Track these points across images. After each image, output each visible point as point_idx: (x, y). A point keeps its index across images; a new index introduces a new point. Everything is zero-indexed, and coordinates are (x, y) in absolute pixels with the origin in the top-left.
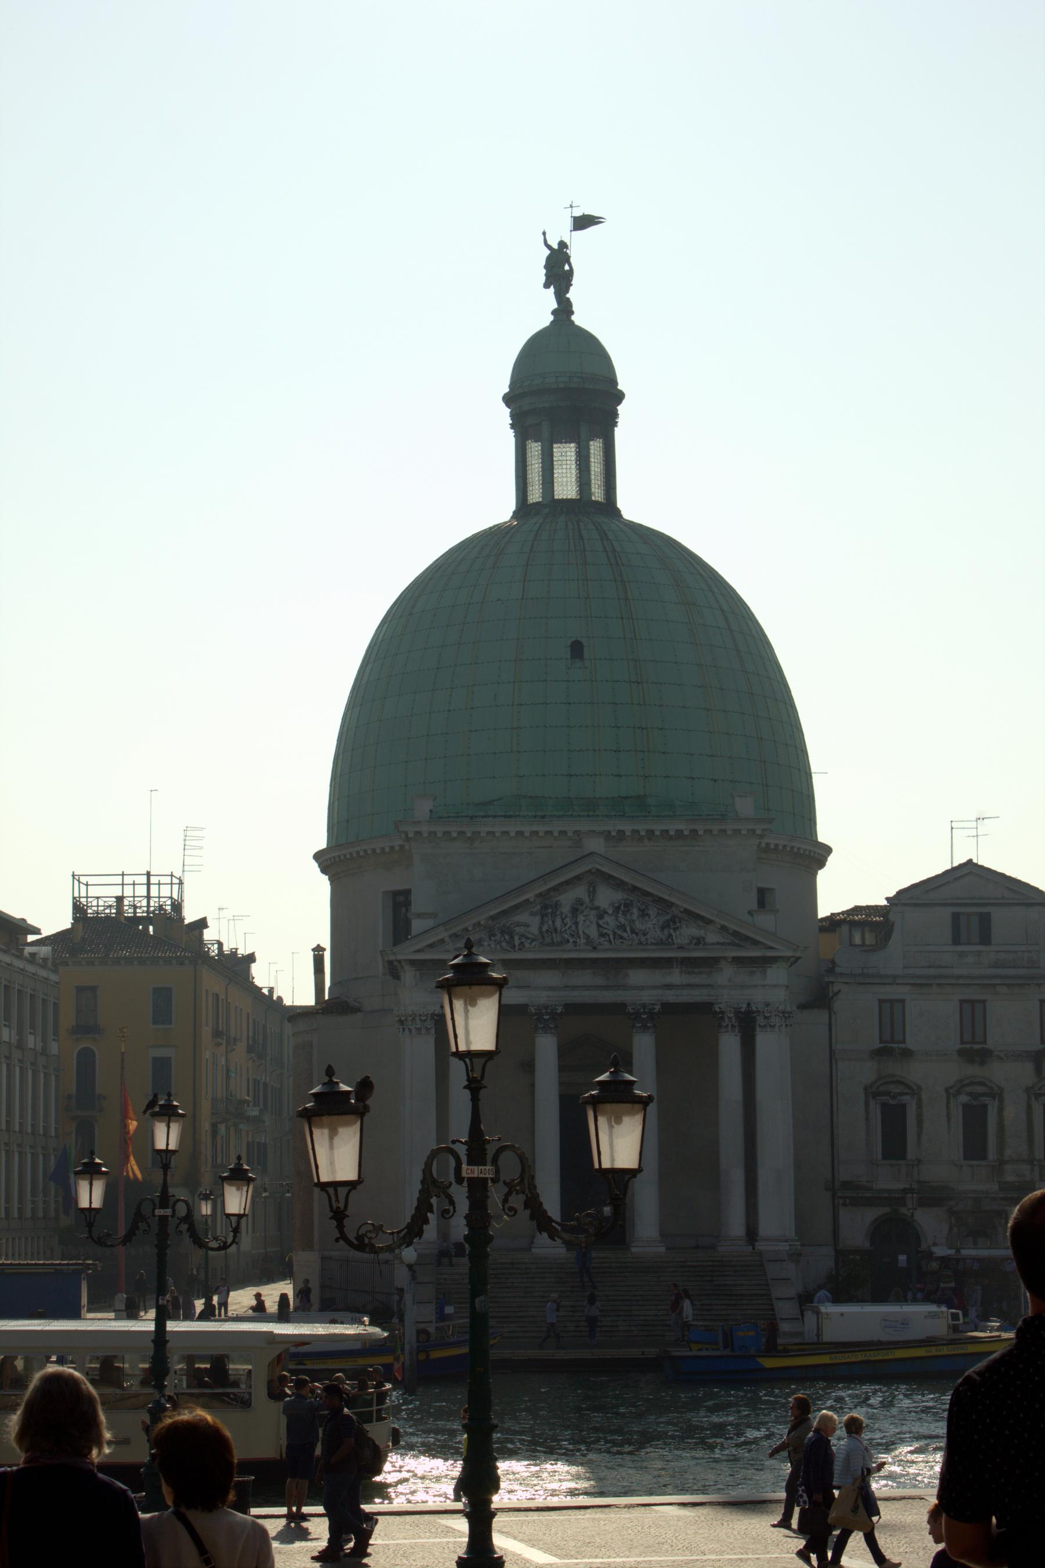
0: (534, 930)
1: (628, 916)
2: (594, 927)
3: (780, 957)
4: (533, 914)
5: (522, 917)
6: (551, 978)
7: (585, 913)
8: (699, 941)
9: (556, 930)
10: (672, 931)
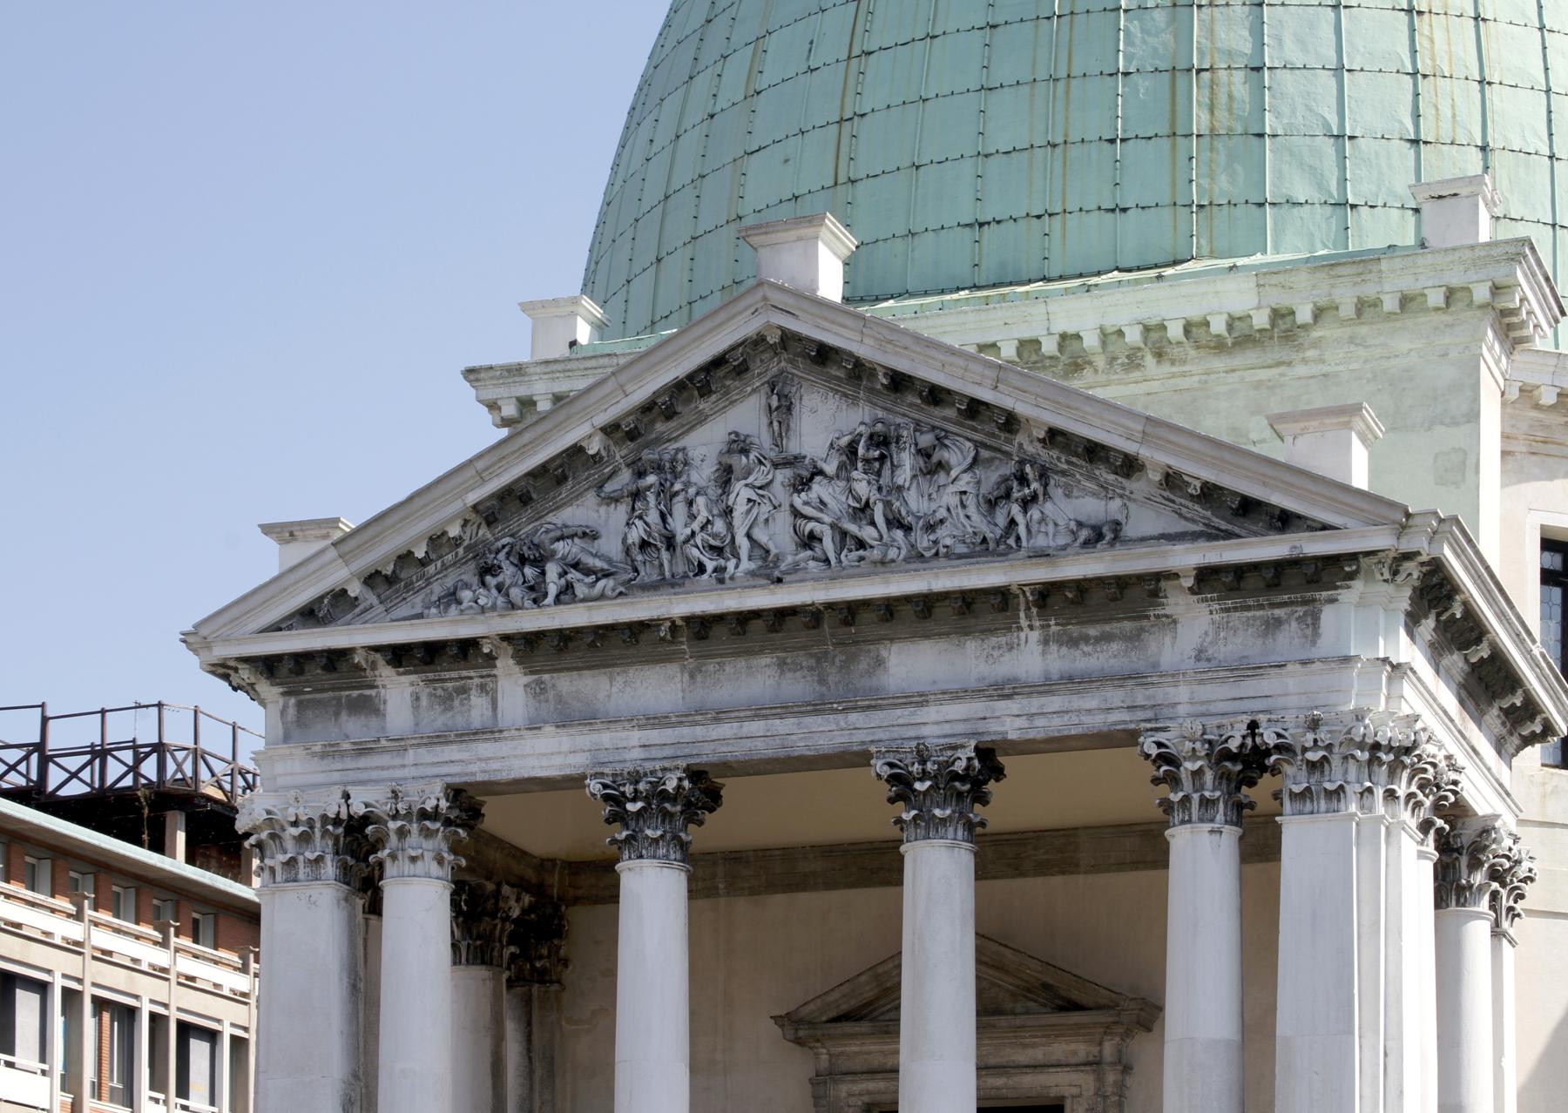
0: (610, 546)
1: (885, 479)
2: (783, 520)
3: (1353, 557)
4: (614, 500)
5: (582, 511)
6: (654, 686)
7: (758, 477)
8: (1098, 535)
9: (670, 542)
10: (1016, 509)
